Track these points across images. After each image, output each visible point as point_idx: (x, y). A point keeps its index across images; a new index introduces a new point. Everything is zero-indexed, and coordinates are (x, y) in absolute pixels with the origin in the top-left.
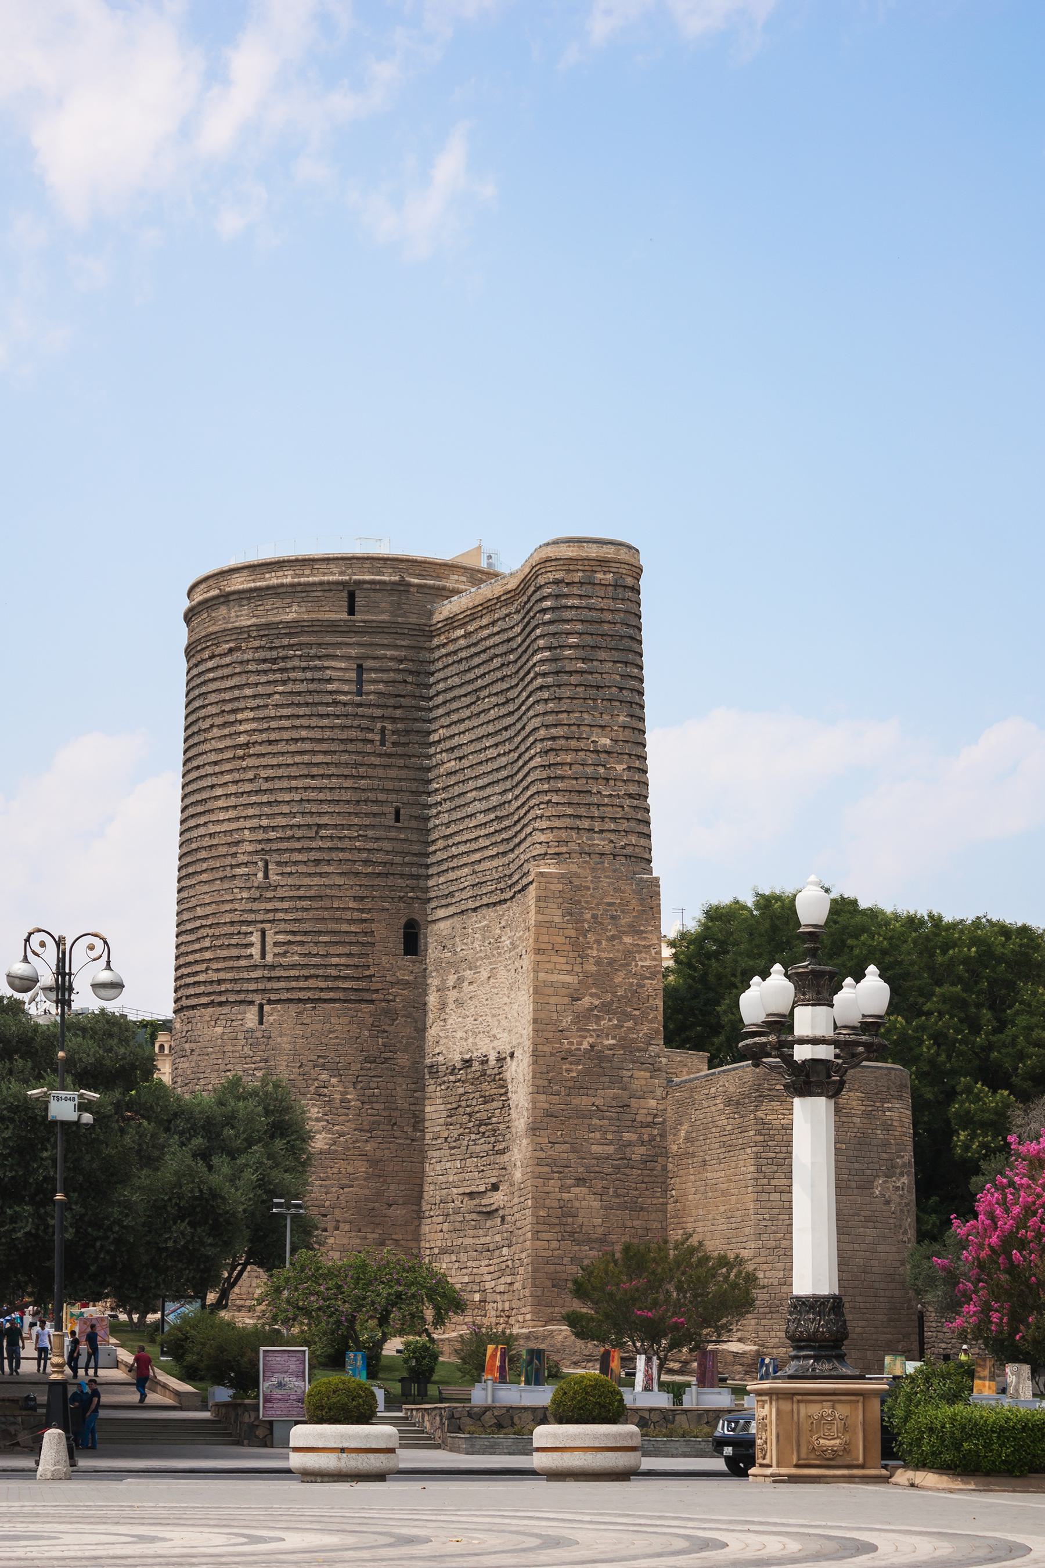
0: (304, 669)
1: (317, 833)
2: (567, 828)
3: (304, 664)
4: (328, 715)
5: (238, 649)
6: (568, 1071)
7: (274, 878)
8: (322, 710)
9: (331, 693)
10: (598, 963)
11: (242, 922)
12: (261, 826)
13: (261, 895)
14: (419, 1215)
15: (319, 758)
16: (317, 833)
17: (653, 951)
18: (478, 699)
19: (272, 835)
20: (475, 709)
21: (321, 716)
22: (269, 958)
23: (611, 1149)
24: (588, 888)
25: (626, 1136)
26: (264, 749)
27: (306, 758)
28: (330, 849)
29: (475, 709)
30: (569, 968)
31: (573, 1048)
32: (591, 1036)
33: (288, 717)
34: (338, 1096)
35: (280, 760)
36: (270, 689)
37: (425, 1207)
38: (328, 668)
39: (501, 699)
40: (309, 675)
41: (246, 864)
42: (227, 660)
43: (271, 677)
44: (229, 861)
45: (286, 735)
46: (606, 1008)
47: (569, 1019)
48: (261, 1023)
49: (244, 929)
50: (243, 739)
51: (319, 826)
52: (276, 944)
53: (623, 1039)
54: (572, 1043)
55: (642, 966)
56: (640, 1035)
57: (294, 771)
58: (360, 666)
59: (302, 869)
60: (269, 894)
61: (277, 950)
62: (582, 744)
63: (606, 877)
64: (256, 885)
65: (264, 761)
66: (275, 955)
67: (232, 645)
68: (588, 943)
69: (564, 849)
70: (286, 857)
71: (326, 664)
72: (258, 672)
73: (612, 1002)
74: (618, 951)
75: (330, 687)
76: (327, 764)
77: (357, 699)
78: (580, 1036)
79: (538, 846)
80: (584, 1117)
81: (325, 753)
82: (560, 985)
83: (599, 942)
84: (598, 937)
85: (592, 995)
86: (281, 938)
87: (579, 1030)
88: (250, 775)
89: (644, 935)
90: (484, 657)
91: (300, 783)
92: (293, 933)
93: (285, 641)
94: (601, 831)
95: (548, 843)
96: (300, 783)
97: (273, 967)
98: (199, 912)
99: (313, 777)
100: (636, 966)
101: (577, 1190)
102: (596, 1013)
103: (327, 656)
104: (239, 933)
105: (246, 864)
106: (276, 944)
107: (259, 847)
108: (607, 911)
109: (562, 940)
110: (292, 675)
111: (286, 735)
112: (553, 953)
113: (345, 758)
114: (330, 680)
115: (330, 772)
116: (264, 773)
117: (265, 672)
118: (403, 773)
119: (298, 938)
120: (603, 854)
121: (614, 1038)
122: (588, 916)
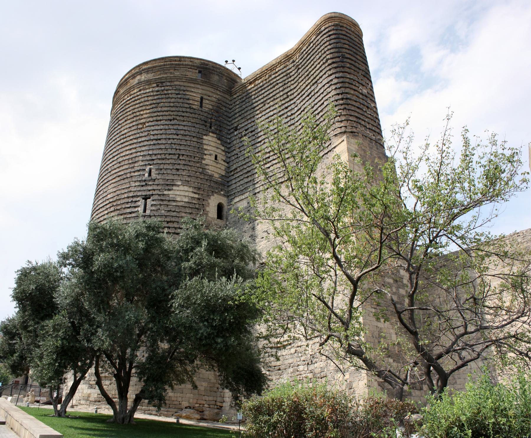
0: (177, 94)
1: (178, 157)
2: (355, 121)
3: (177, 92)
4: (187, 112)
5: (144, 89)
7: (154, 175)
8: (184, 110)
9: (189, 104)
11: (132, 197)
12: (149, 154)
13: (146, 184)
15: (181, 127)
16: (178, 157)
18: (265, 105)
19: (155, 158)
20: (264, 108)
21: (183, 112)
22: (148, 212)
26: (153, 123)
27: (175, 127)
28: (184, 165)
29: (264, 108)
33: (167, 111)
35: (162, 127)
36: (158, 101)
38: (188, 95)
39: (285, 96)
40: (179, 96)
41: (139, 171)
42: (138, 94)
43: (159, 97)
44: (130, 170)
45: (165, 118)
49: (134, 199)
50: (142, 121)
51: (179, 155)
52: (152, 205)
57: (168, 132)
58: (202, 99)
59: (169, 171)
60: (150, 183)
61: (154, 208)
62: (356, 88)
64: (143, 179)
65: (152, 128)
67: (141, 88)
69: (354, 130)
70: (162, 166)
71: (187, 93)
72: (154, 96)
75: (188, 102)
76: (185, 130)
77: (200, 109)
79: (339, 129)
81: (184, 126)
86: (154, 203)
88: (146, 134)
90: (271, 86)
91: (171, 136)
92: (162, 200)
93: (168, 84)
94: (369, 129)
95: (346, 127)
96: (171, 136)
97: (150, 216)
98: (109, 196)
99: (178, 135)
103: (188, 91)
104: (132, 201)
105: (139, 171)
107: (147, 163)
110: (170, 96)
111: (165, 118)
113: (193, 129)
114: (188, 99)
115: (186, 134)
116: (152, 133)
117: (157, 95)
118: (219, 142)
119: (165, 203)
120: (371, 139)
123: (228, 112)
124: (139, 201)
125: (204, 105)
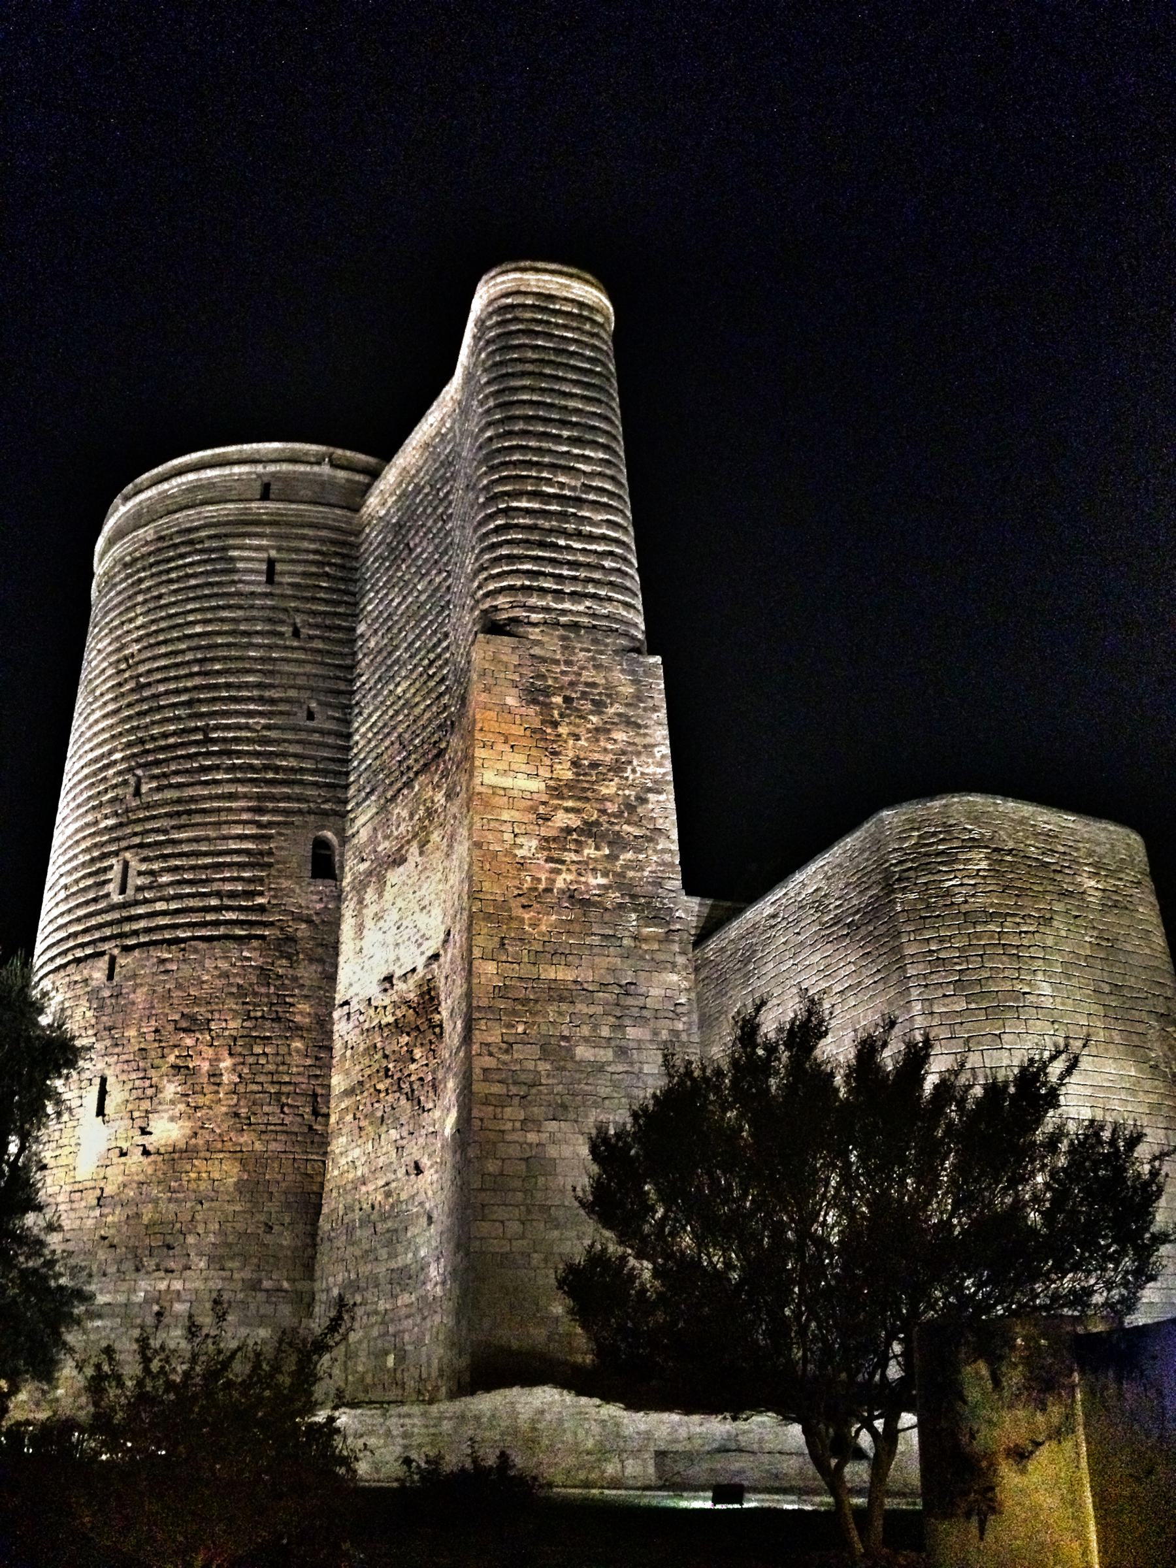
6: (534, 925)
10: (575, 763)
14: (311, 1239)
17: (658, 755)
22: (130, 892)
23: (607, 1055)
24: (557, 662)
25: (632, 1033)
30: (531, 769)
31: (541, 887)
32: (568, 870)
34: (205, 1066)
37: (324, 1225)
46: (589, 830)
47: (534, 843)
48: (110, 977)
52: (140, 873)
53: (622, 875)
54: (539, 880)
55: (642, 774)
56: (646, 874)
58: (271, 563)
63: (582, 650)
66: (139, 889)
68: (560, 736)
73: (597, 823)
74: (605, 750)
78: (552, 871)
80: (561, 999)
82: (515, 793)
83: (577, 738)
84: (577, 731)
85: (568, 810)
87: (549, 860)
89: (642, 731)
100: (634, 771)
101: (553, 1126)
102: (575, 836)
106: (140, 873)
108: (584, 693)
109: (518, 731)
112: (507, 748)
121: (605, 874)
122: (558, 700)
123: (351, 580)
124: (111, 867)
125: (277, 579)
